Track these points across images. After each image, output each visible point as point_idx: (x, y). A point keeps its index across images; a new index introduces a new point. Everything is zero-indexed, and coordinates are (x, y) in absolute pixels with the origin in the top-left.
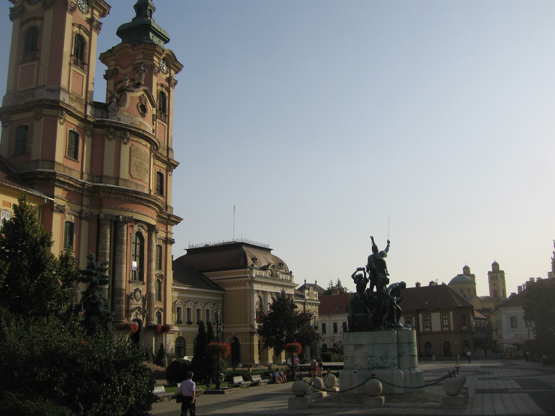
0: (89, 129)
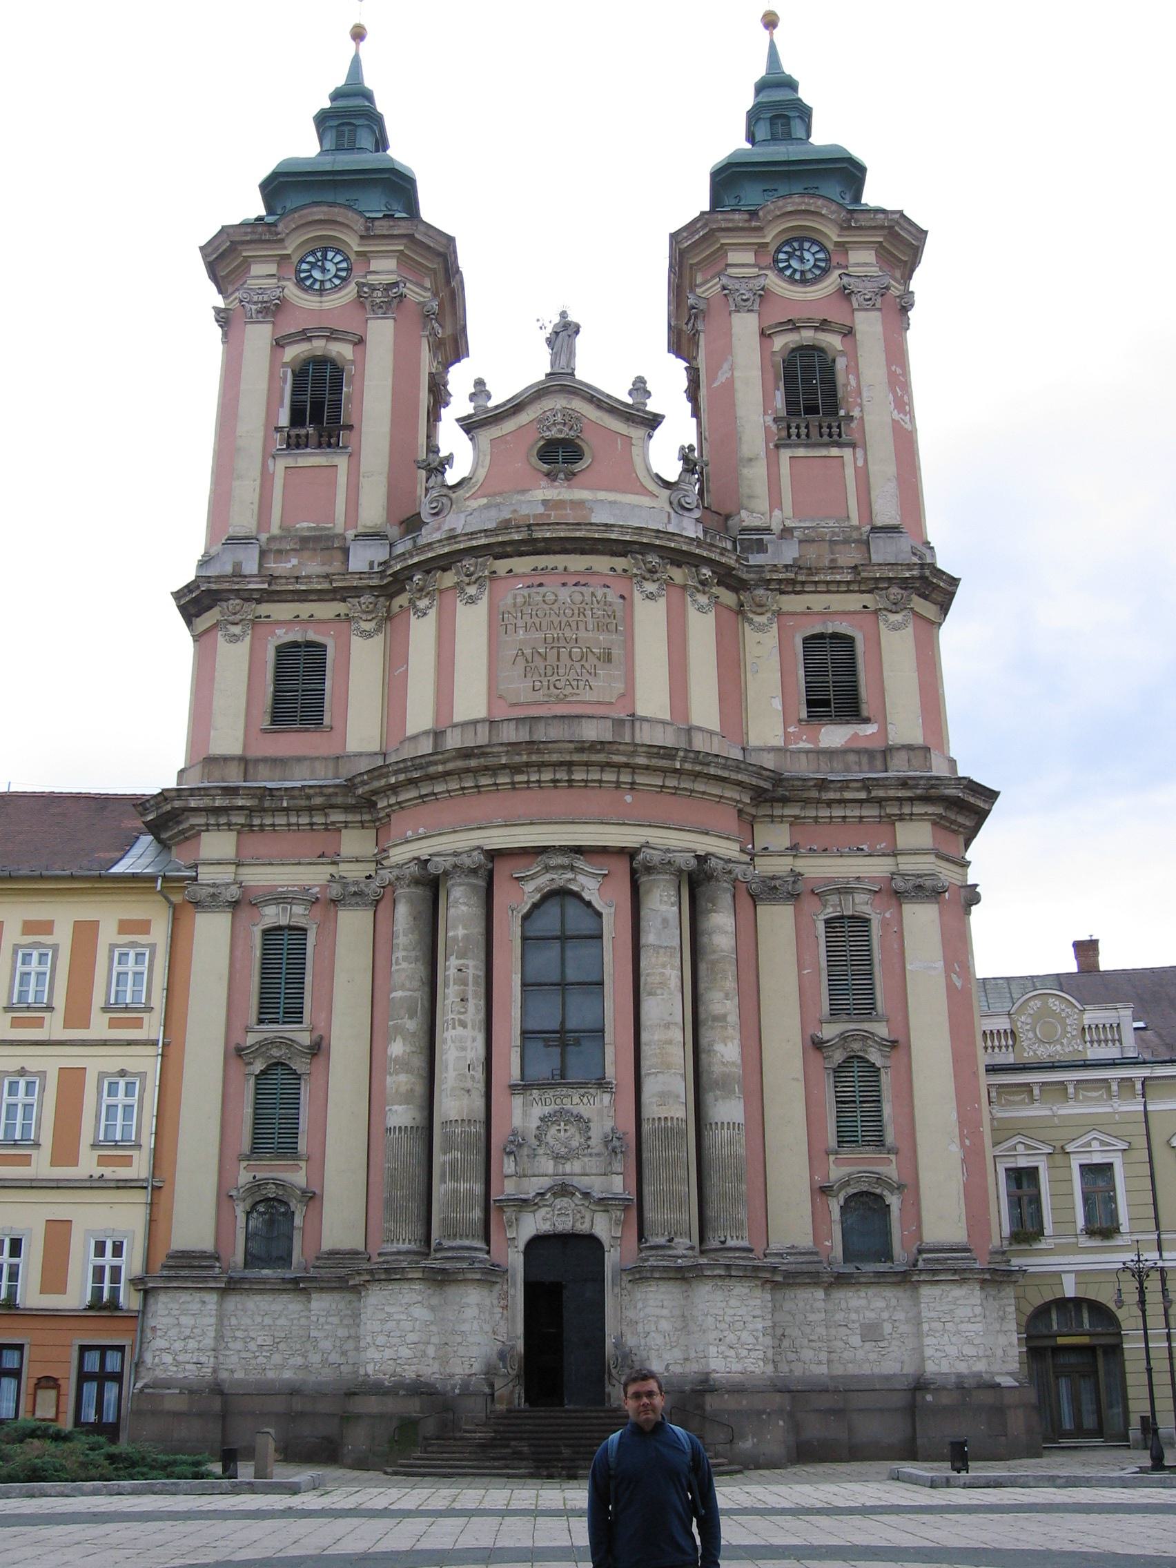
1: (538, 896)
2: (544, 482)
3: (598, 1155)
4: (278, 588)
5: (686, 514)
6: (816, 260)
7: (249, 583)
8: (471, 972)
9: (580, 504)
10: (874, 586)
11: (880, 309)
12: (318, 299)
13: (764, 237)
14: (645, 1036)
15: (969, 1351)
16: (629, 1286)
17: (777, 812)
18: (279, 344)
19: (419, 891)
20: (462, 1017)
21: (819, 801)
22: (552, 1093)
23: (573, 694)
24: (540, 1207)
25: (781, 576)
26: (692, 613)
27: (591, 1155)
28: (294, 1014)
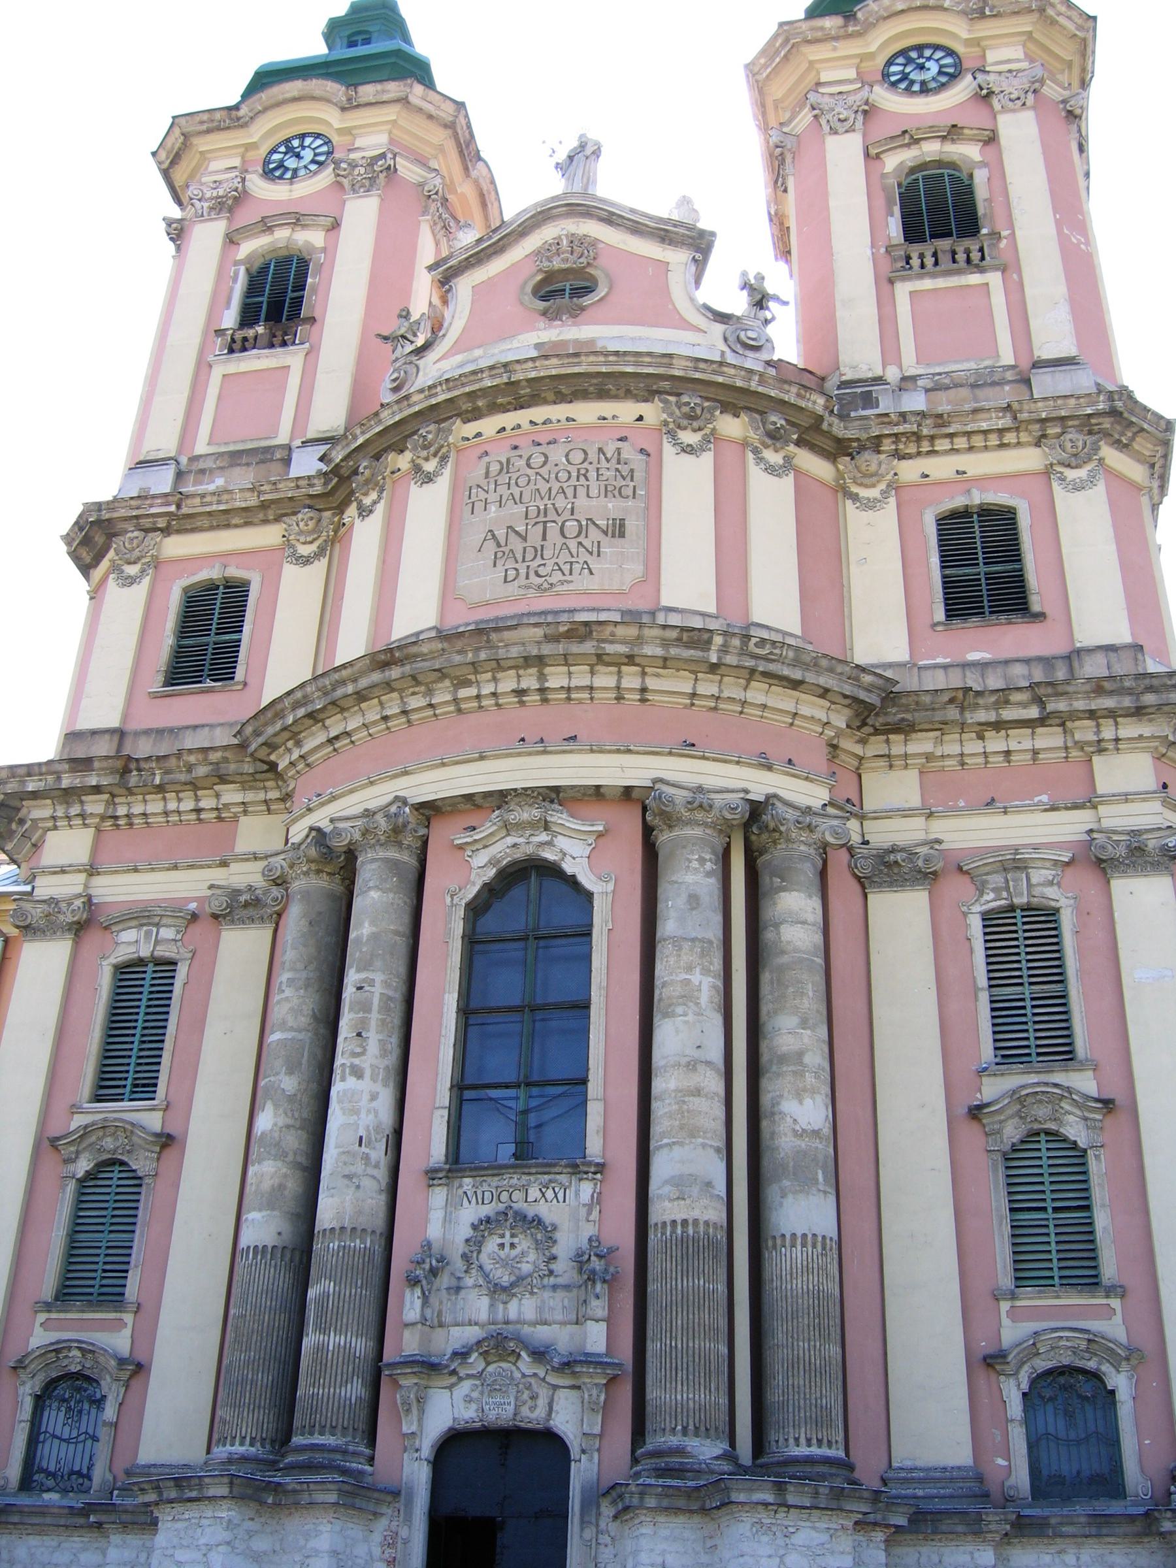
0: (301, 532)
1: (492, 872)
2: (542, 323)
3: (567, 1287)
4: (191, 511)
6: (941, 67)
7: (151, 506)
8: (378, 990)
14: (659, 1085)
16: (613, 1527)
17: (897, 749)
18: (231, 240)
19: (322, 883)
20: (356, 1061)
21: (963, 726)
22: (495, 1181)
23: (562, 582)
24: (460, 1379)
26: (756, 474)
27: (555, 1287)
28: (145, 1087)
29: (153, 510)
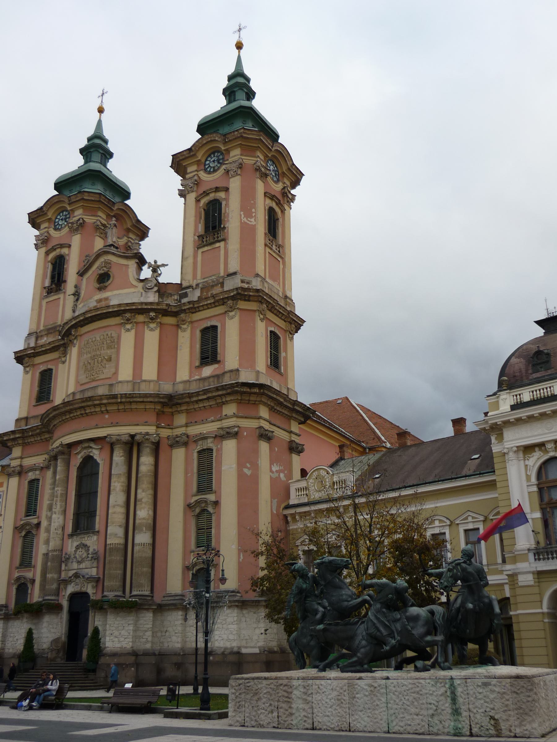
1: (82, 459)
2: (98, 292)
5: (150, 291)
9: (107, 299)
10: (223, 302)
11: (239, 174)
12: (59, 232)
13: (198, 157)
15: (231, 637)
25: (188, 307)
29: (29, 352)
